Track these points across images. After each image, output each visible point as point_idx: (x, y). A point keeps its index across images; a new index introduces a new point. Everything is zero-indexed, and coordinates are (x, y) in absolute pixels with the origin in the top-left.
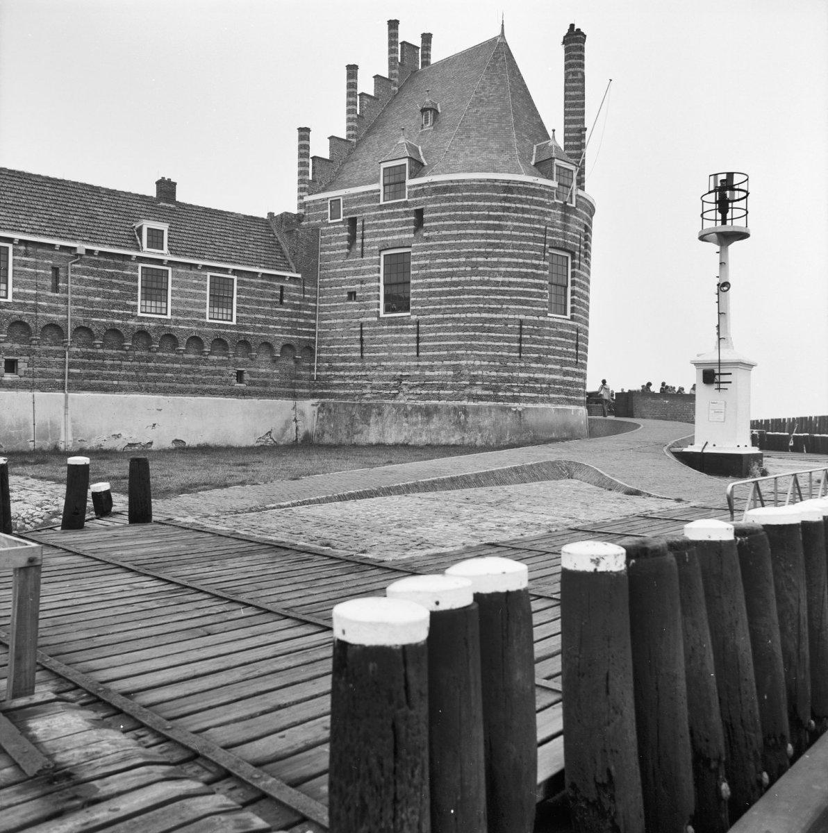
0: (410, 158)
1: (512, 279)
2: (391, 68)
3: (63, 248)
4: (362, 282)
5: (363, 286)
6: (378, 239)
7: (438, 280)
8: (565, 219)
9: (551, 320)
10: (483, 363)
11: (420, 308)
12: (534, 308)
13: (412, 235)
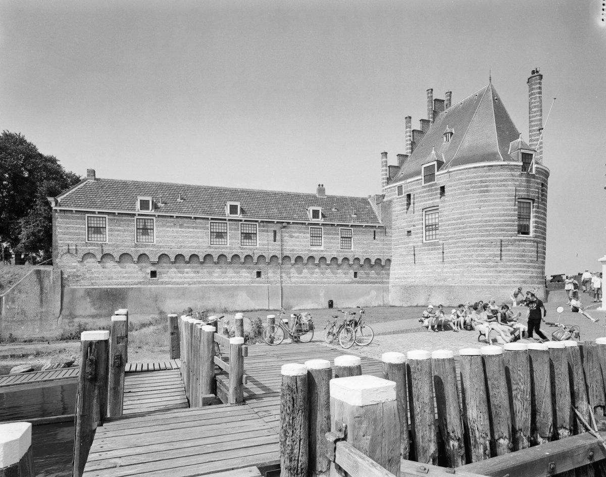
0: (437, 161)
2: (429, 114)
3: (278, 222)
4: (414, 226)
5: (415, 228)
6: (422, 203)
7: (454, 222)
8: (528, 181)
9: (520, 238)
10: (479, 264)
11: (444, 237)
13: (439, 200)
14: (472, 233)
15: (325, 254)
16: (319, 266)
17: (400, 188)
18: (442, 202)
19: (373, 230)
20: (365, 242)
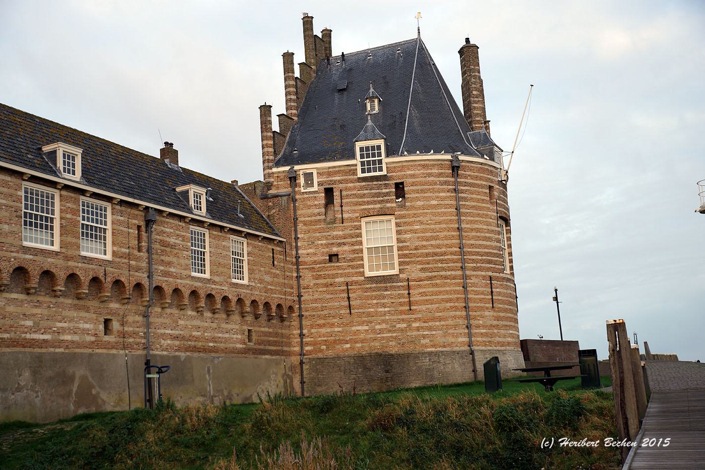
1: (481, 242)
12: (497, 266)
14: (454, 263)
15: (214, 288)
16: (202, 315)
17: (309, 177)
18: (402, 206)
19: (270, 247)
20: (262, 269)
